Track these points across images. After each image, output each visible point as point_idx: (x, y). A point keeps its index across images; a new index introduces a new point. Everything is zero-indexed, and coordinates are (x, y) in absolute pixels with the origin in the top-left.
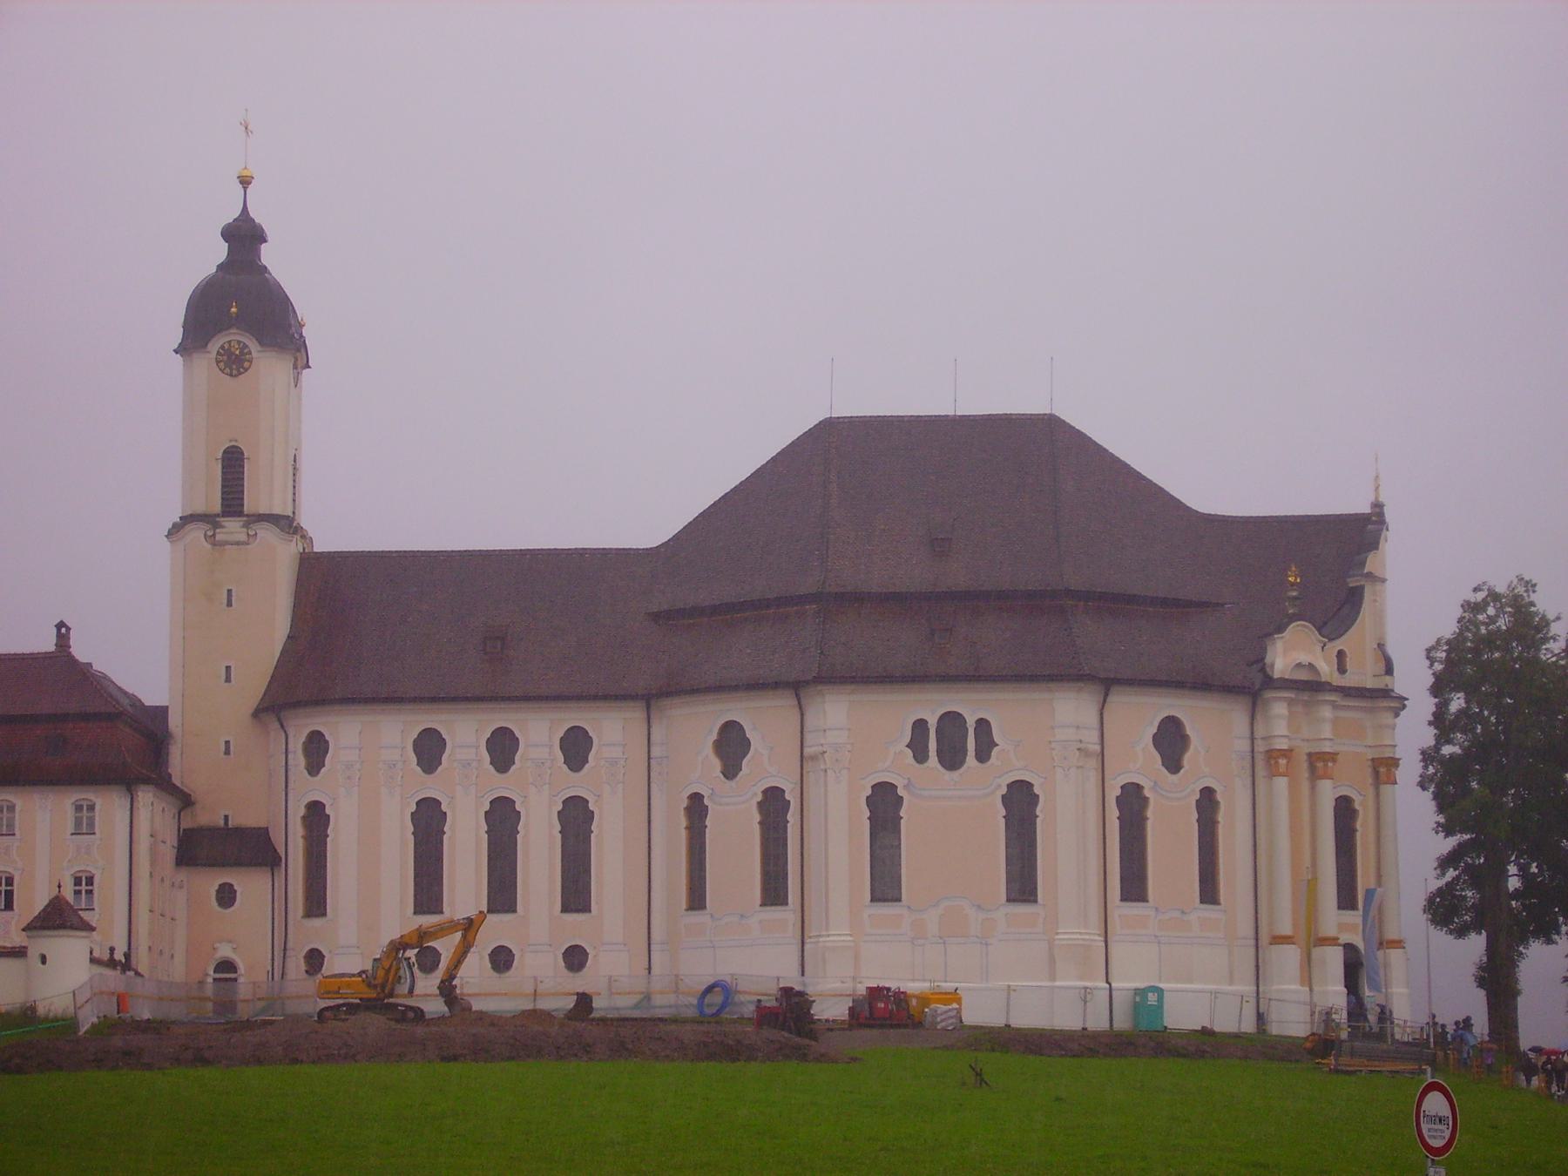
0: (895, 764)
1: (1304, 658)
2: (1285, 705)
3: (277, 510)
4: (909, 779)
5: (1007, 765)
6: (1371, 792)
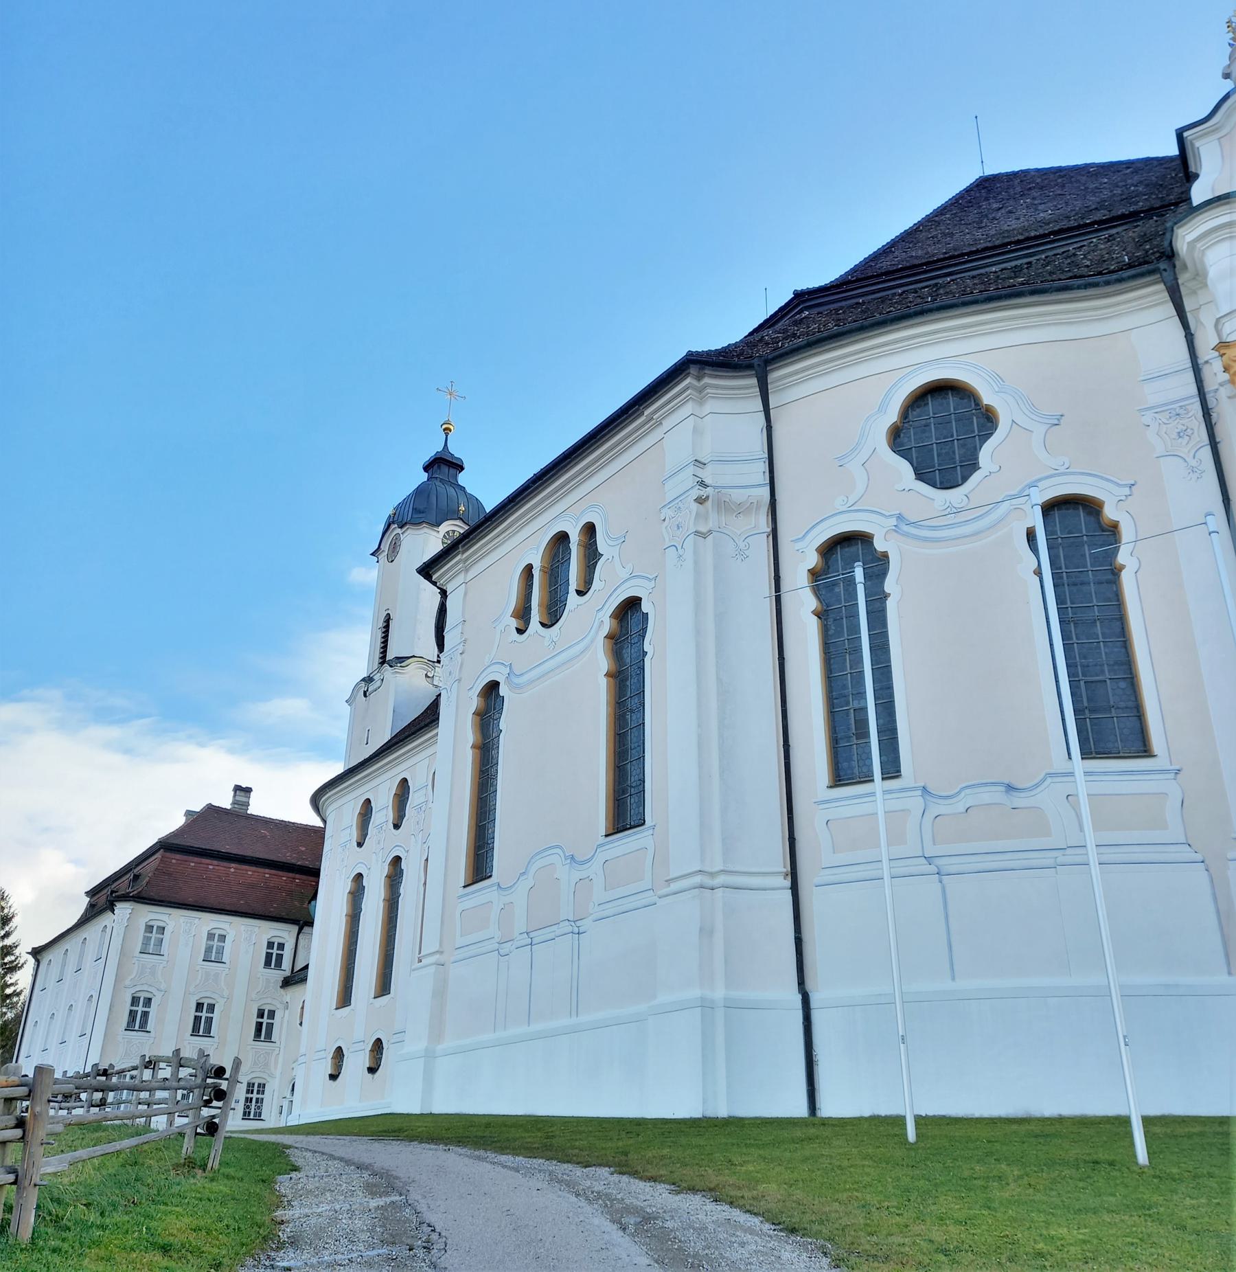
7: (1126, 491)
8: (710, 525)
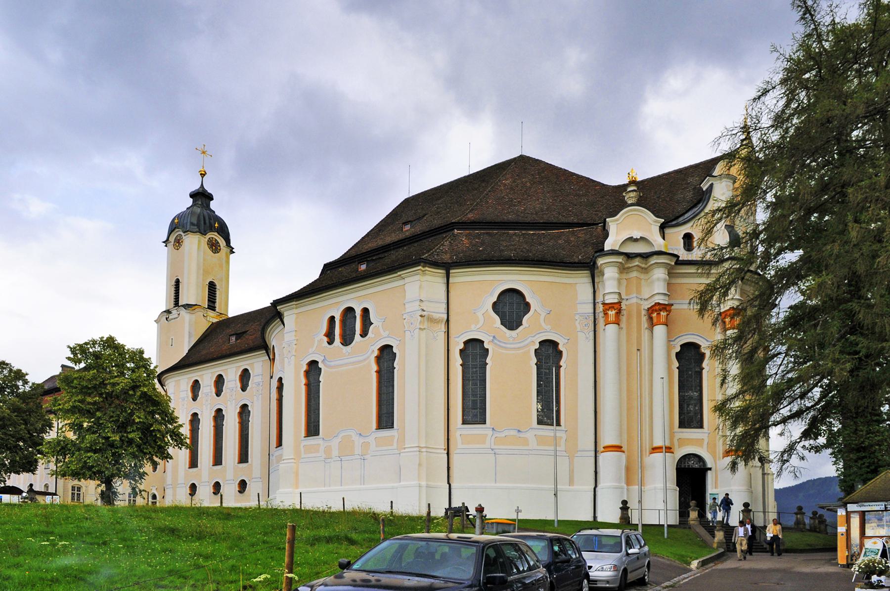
3: (192, 302)
5: (378, 336)
7: (566, 341)
8: (425, 327)
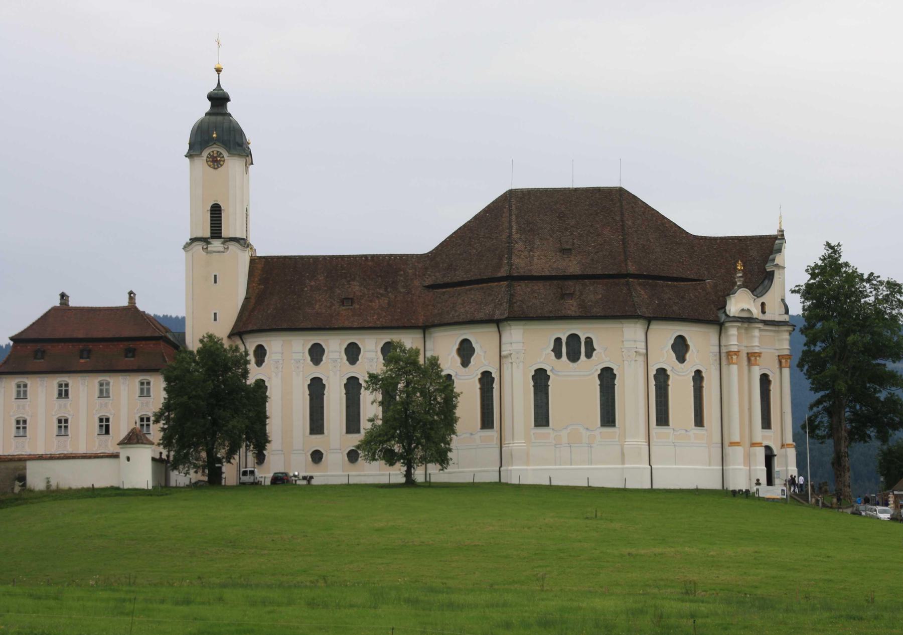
0: (546, 360)
1: (746, 307)
2: (736, 329)
3: (238, 235)
4: (553, 367)
5: (600, 360)
6: (778, 371)
